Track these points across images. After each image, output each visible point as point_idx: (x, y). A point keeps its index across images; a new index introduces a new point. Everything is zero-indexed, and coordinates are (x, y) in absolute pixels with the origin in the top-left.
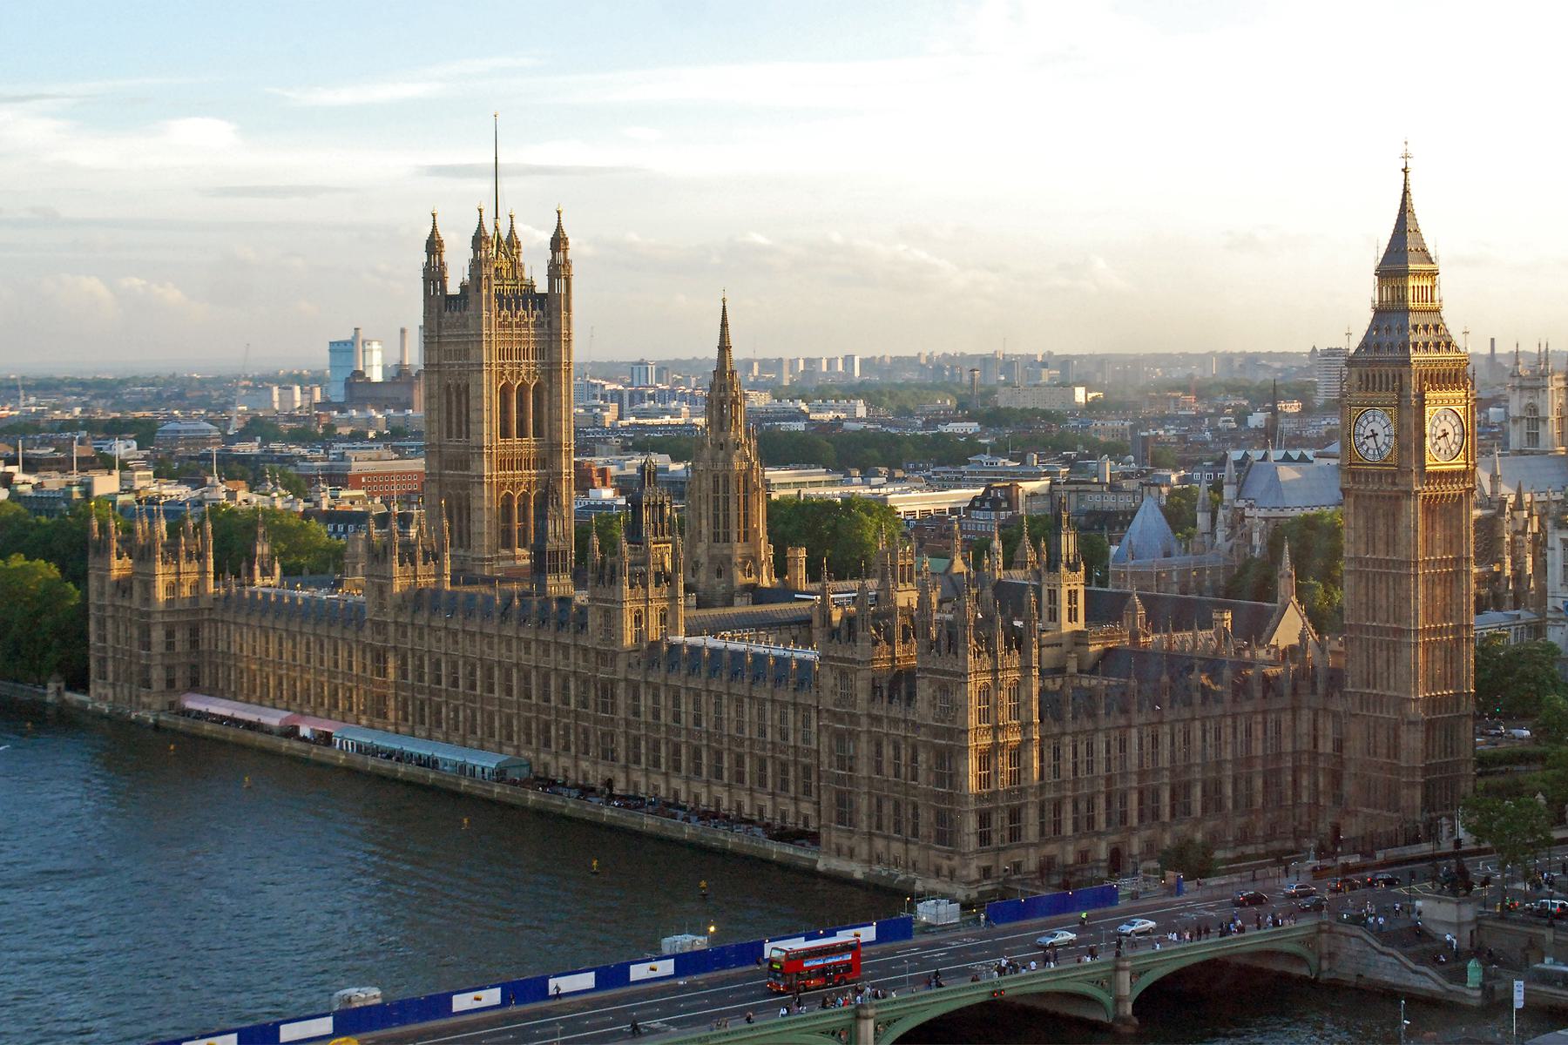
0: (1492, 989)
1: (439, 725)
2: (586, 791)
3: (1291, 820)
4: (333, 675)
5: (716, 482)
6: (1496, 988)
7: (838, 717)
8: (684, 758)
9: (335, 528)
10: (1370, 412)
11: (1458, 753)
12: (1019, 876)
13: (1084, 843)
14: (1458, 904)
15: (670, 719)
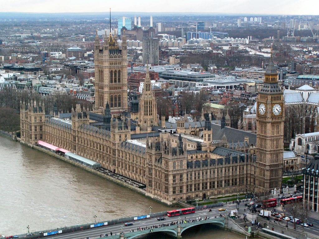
0: (253, 233)
1: (85, 153)
2: (110, 171)
3: (245, 188)
4: (66, 139)
5: (145, 103)
6: (254, 232)
7: (149, 165)
8: (127, 167)
9: (83, 95)
10: (261, 104)
11: (279, 176)
12: (182, 200)
13: (197, 193)
14: (253, 214)
15: (125, 158)
